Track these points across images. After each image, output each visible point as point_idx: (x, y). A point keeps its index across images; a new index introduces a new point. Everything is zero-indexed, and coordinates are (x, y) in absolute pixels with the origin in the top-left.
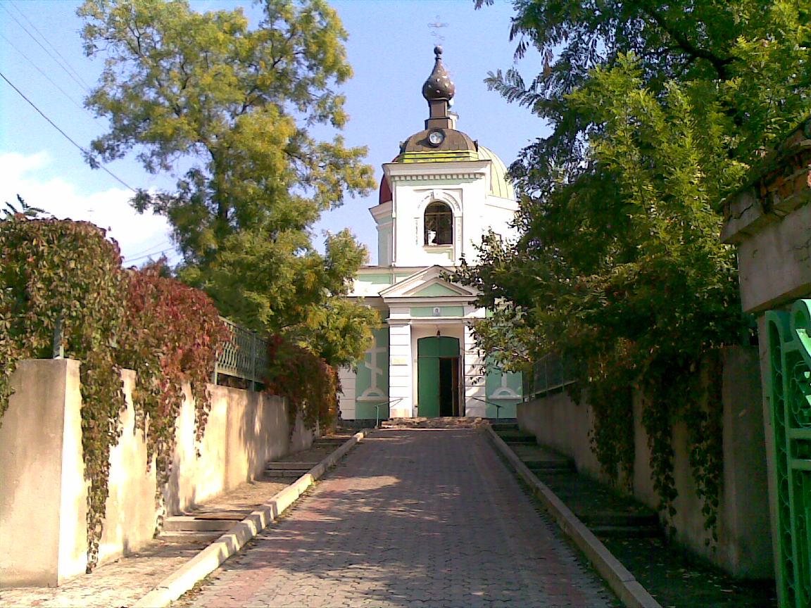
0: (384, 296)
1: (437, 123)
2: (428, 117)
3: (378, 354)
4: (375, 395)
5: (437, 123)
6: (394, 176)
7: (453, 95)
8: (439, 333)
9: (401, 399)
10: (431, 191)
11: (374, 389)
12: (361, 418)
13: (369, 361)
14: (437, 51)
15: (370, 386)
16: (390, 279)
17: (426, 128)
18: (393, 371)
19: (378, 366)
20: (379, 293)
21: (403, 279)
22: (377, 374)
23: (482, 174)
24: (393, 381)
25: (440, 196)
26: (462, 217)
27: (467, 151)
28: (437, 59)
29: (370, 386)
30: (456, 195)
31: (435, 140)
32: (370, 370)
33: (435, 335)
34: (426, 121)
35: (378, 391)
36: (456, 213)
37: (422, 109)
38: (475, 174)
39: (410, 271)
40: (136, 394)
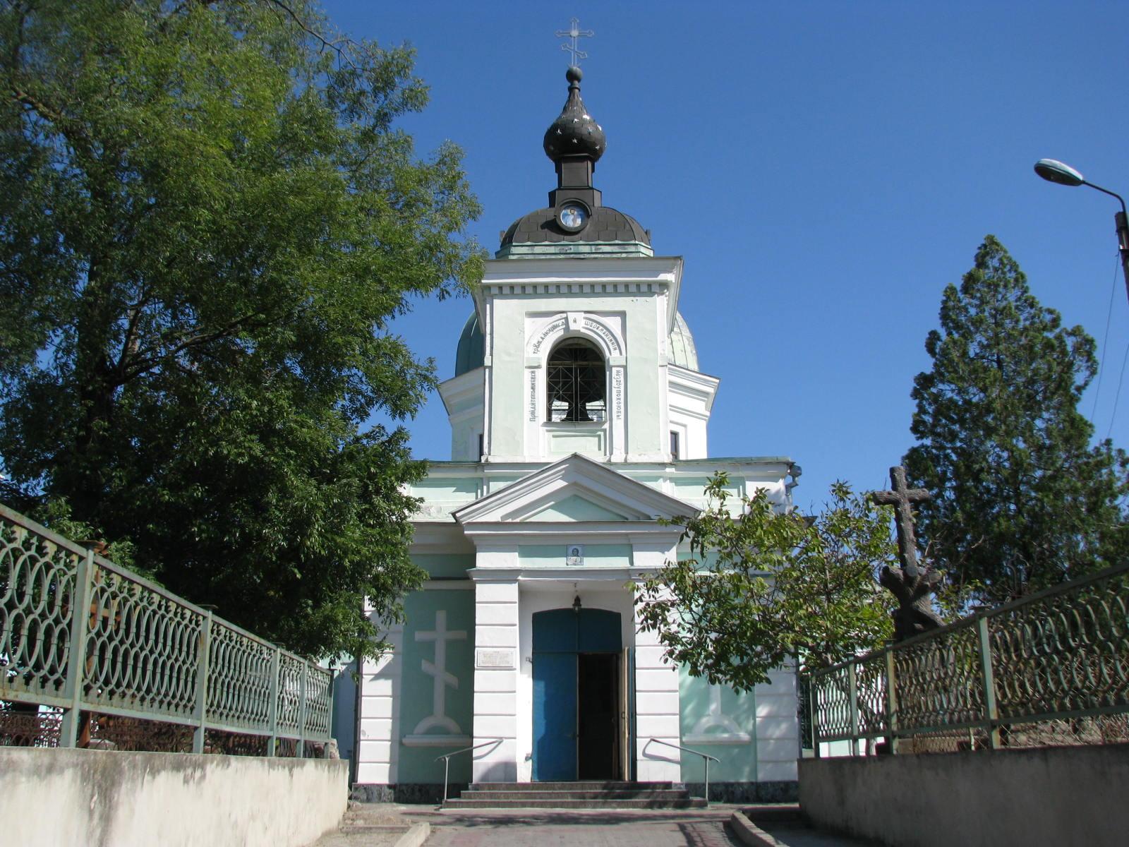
0: (465, 521)
3: (450, 644)
6: (488, 287)
8: (578, 600)
9: (500, 743)
10: (564, 315)
11: (439, 717)
13: (432, 661)
14: (572, 76)
15: (431, 713)
16: (474, 485)
17: (552, 204)
19: (449, 668)
20: (454, 514)
21: (502, 485)
22: (448, 687)
23: (664, 285)
24: (481, 703)
25: (580, 325)
26: (625, 368)
27: (633, 242)
28: (571, 89)
29: (431, 713)
30: (614, 324)
31: (571, 219)
32: (431, 678)
33: (569, 604)
34: (552, 195)
35: (451, 724)
36: (613, 357)
38: (650, 285)
39: (520, 472)
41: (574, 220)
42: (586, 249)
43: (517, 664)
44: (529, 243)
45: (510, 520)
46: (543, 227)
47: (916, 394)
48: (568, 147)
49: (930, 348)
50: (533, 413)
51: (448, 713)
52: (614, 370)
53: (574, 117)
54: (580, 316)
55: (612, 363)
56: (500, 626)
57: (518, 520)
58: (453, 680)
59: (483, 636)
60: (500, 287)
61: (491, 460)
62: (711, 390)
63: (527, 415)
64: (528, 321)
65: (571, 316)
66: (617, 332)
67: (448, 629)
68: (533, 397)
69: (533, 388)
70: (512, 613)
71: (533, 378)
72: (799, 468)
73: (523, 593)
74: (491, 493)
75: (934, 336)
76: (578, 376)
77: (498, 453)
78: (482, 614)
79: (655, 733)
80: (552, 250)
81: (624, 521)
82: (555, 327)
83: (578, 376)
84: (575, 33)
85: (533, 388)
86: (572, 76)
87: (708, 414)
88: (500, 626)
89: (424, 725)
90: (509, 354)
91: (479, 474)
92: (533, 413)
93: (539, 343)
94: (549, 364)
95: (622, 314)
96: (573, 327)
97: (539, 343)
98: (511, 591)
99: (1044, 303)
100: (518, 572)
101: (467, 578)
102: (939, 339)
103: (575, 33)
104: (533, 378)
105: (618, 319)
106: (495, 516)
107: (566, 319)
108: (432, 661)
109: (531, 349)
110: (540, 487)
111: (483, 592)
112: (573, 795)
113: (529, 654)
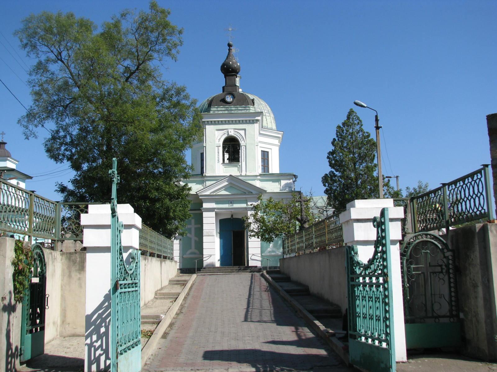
1: (230, 88)
2: (224, 85)
3: (196, 229)
4: (195, 253)
5: (230, 88)
6: (204, 122)
7: (239, 71)
8: (232, 216)
10: (227, 130)
11: (193, 250)
12: (186, 267)
13: (190, 233)
14: (230, 45)
15: (191, 248)
16: (202, 182)
17: (223, 91)
18: (205, 239)
19: (196, 236)
20: (196, 193)
22: (195, 241)
23: (258, 120)
24: (205, 245)
25: (232, 133)
26: (246, 146)
27: (248, 106)
28: (229, 50)
29: (191, 248)
30: (242, 132)
31: (229, 99)
32: (190, 239)
33: (230, 217)
34: (223, 88)
35: (196, 251)
36: (242, 143)
37: (221, 79)
38: (253, 120)
40: (137, 281)
41: (230, 99)
42: (234, 109)
43: (215, 235)
44: (216, 107)
45: (212, 194)
46: (220, 101)
47: (328, 157)
48: (229, 71)
49: (333, 143)
50: (218, 160)
51: (196, 248)
52: (242, 147)
53: (230, 61)
54: (232, 130)
55: (242, 145)
56: (210, 223)
57: (214, 194)
58: (197, 239)
59: (205, 227)
60: (208, 121)
61: (207, 175)
62: (280, 136)
63: (217, 161)
64: (216, 132)
65: (229, 130)
66: (243, 135)
67: (195, 224)
68: (218, 155)
69: (218, 153)
70: (213, 220)
71: (218, 150)
72: (297, 176)
73: (216, 214)
74: (207, 186)
75: (334, 140)
76: (232, 148)
77: (208, 172)
78: (205, 221)
79: (254, 253)
80: (223, 109)
81: (245, 194)
82: (225, 134)
83: (232, 148)
84: (230, 29)
85: (218, 153)
86: (230, 45)
87: (279, 144)
88: (210, 223)
89: (189, 252)
90: (211, 142)
91: (203, 179)
92: (218, 160)
93: (220, 139)
94: (223, 145)
95: (245, 130)
96: (230, 134)
97: (220, 139)
98: (213, 214)
99: (365, 131)
100: (215, 208)
101: (200, 210)
102: (336, 141)
103: (230, 29)
104: (218, 150)
105: (244, 131)
106: (208, 193)
107: (228, 131)
108: (190, 233)
109: (218, 141)
110: (221, 184)
111: (204, 213)
112: (231, 270)
113: (219, 231)
